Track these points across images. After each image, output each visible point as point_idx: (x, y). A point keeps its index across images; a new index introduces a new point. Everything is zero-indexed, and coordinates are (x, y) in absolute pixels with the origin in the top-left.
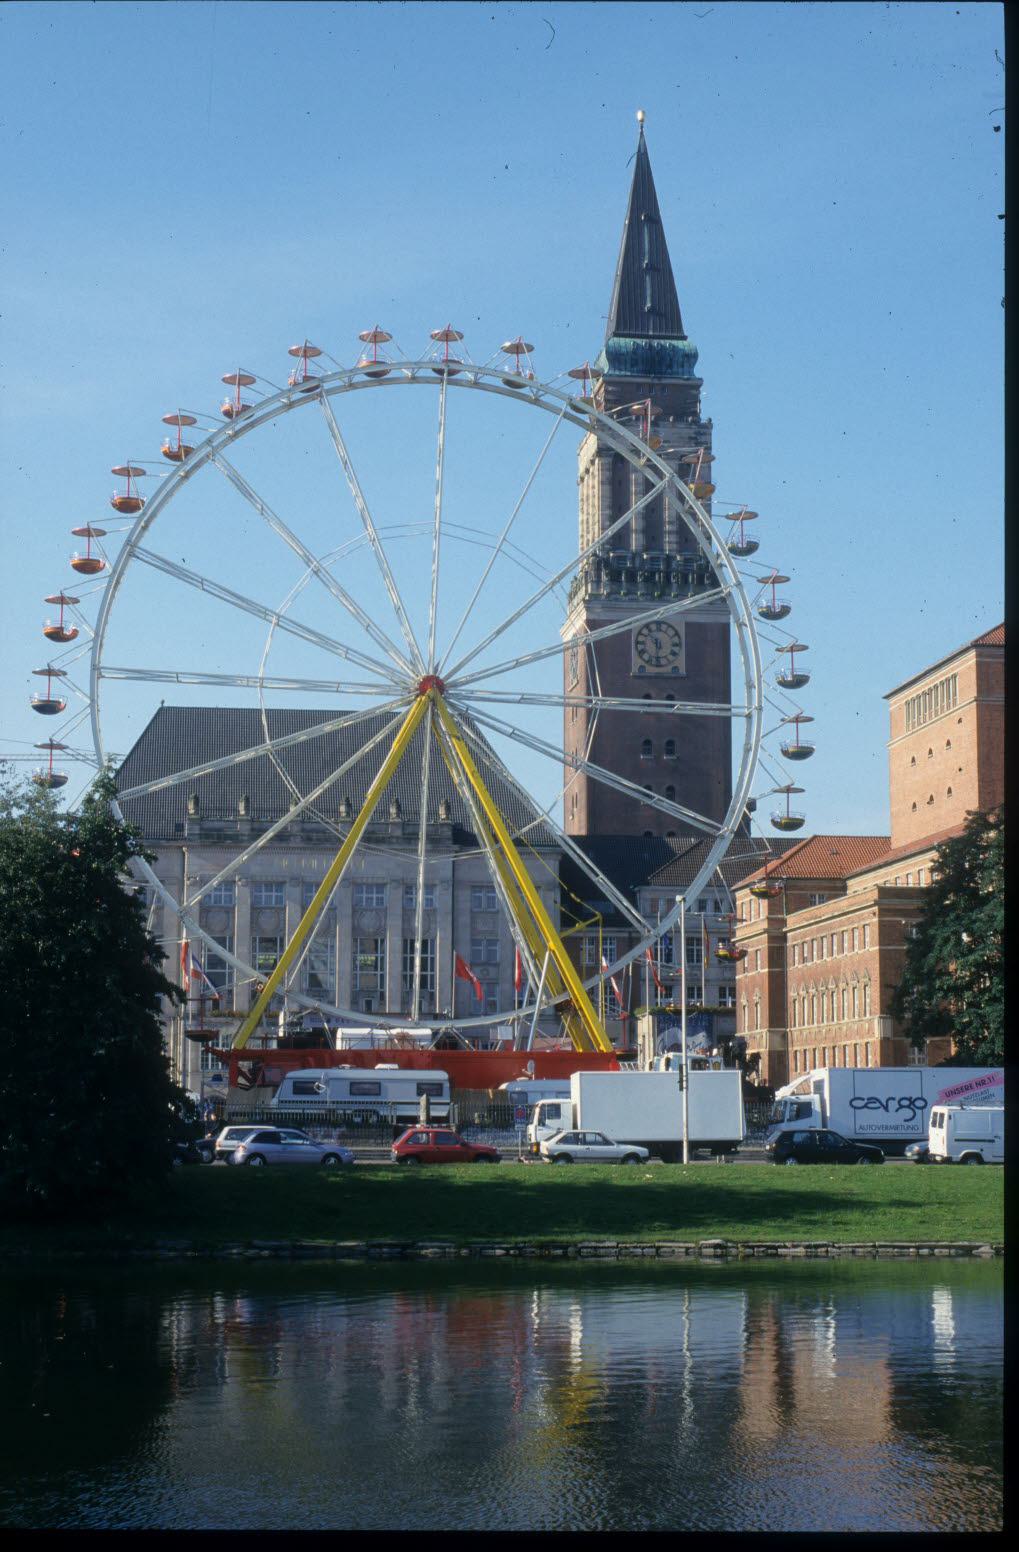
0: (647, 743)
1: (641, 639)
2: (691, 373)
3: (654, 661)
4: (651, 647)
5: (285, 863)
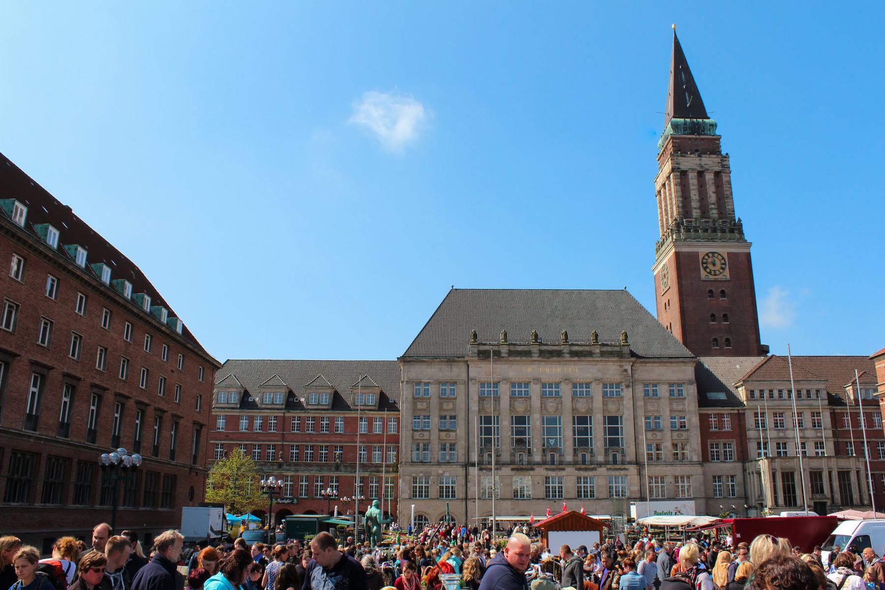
0: (713, 315)
4: (711, 267)
5: (529, 370)
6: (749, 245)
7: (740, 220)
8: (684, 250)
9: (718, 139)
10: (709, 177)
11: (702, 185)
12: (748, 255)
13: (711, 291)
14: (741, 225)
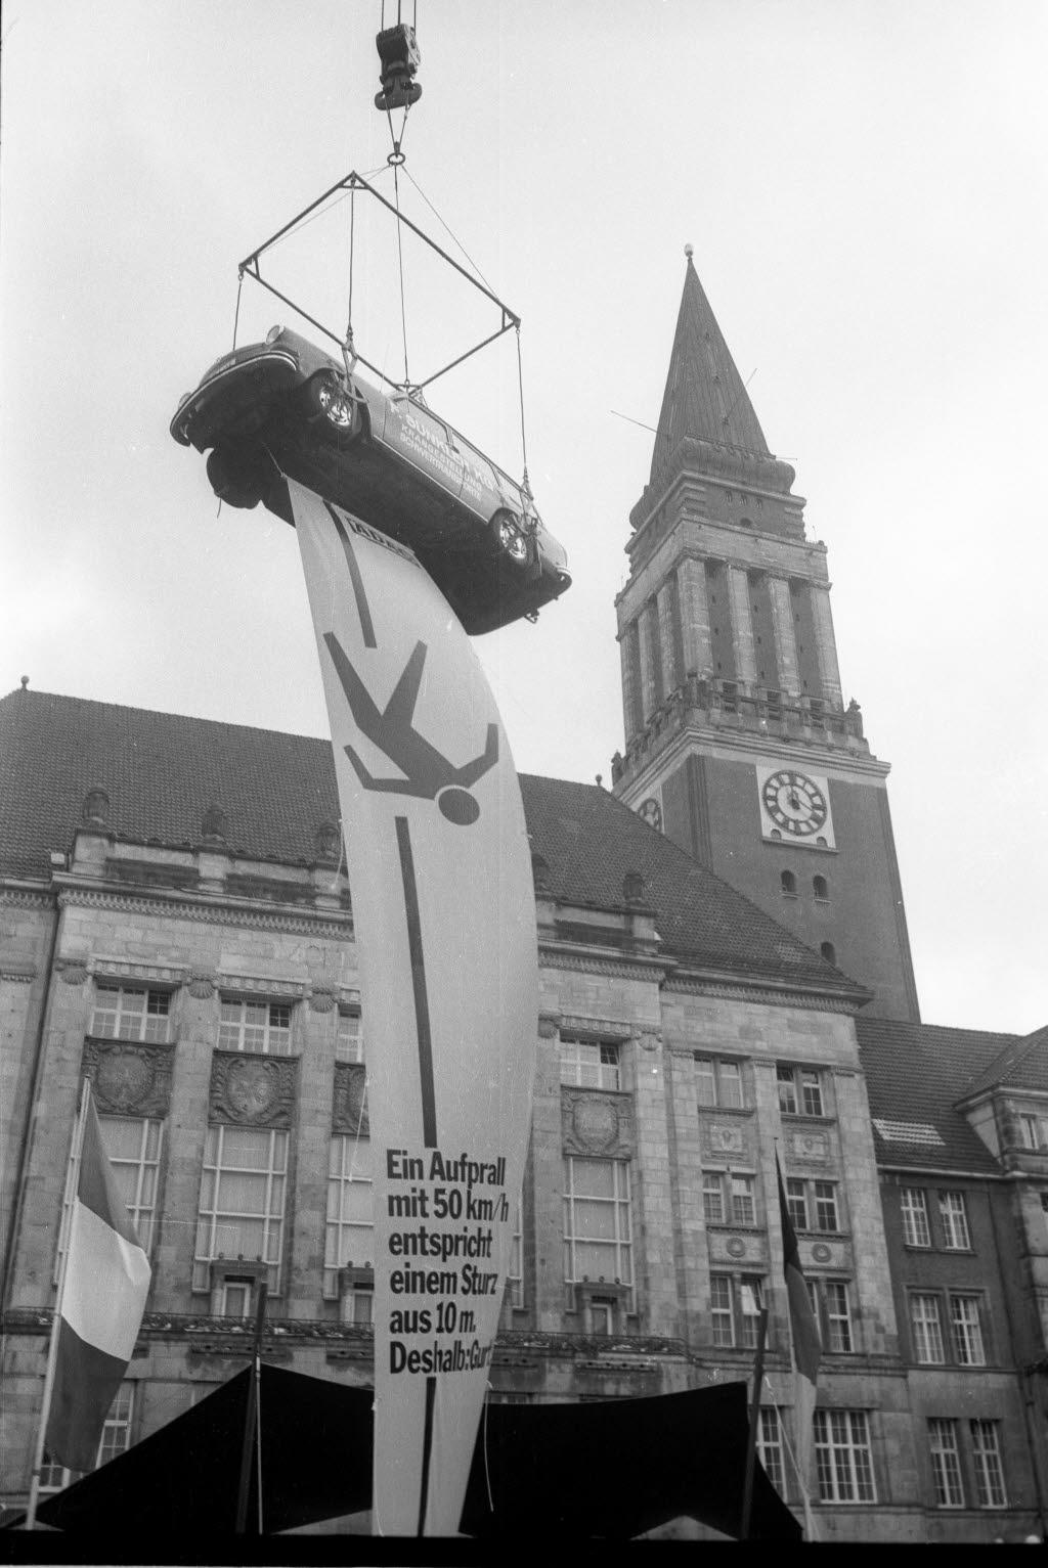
1: (771, 792)
2: (786, 492)
3: (791, 826)
6: (883, 770)
7: (854, 706)
8: (717, 753)
9: (800, 504)
10: (779, 590)
11: (761, 608)
12: (882, 795)
13: (787, 878)
14: (859, 717)
